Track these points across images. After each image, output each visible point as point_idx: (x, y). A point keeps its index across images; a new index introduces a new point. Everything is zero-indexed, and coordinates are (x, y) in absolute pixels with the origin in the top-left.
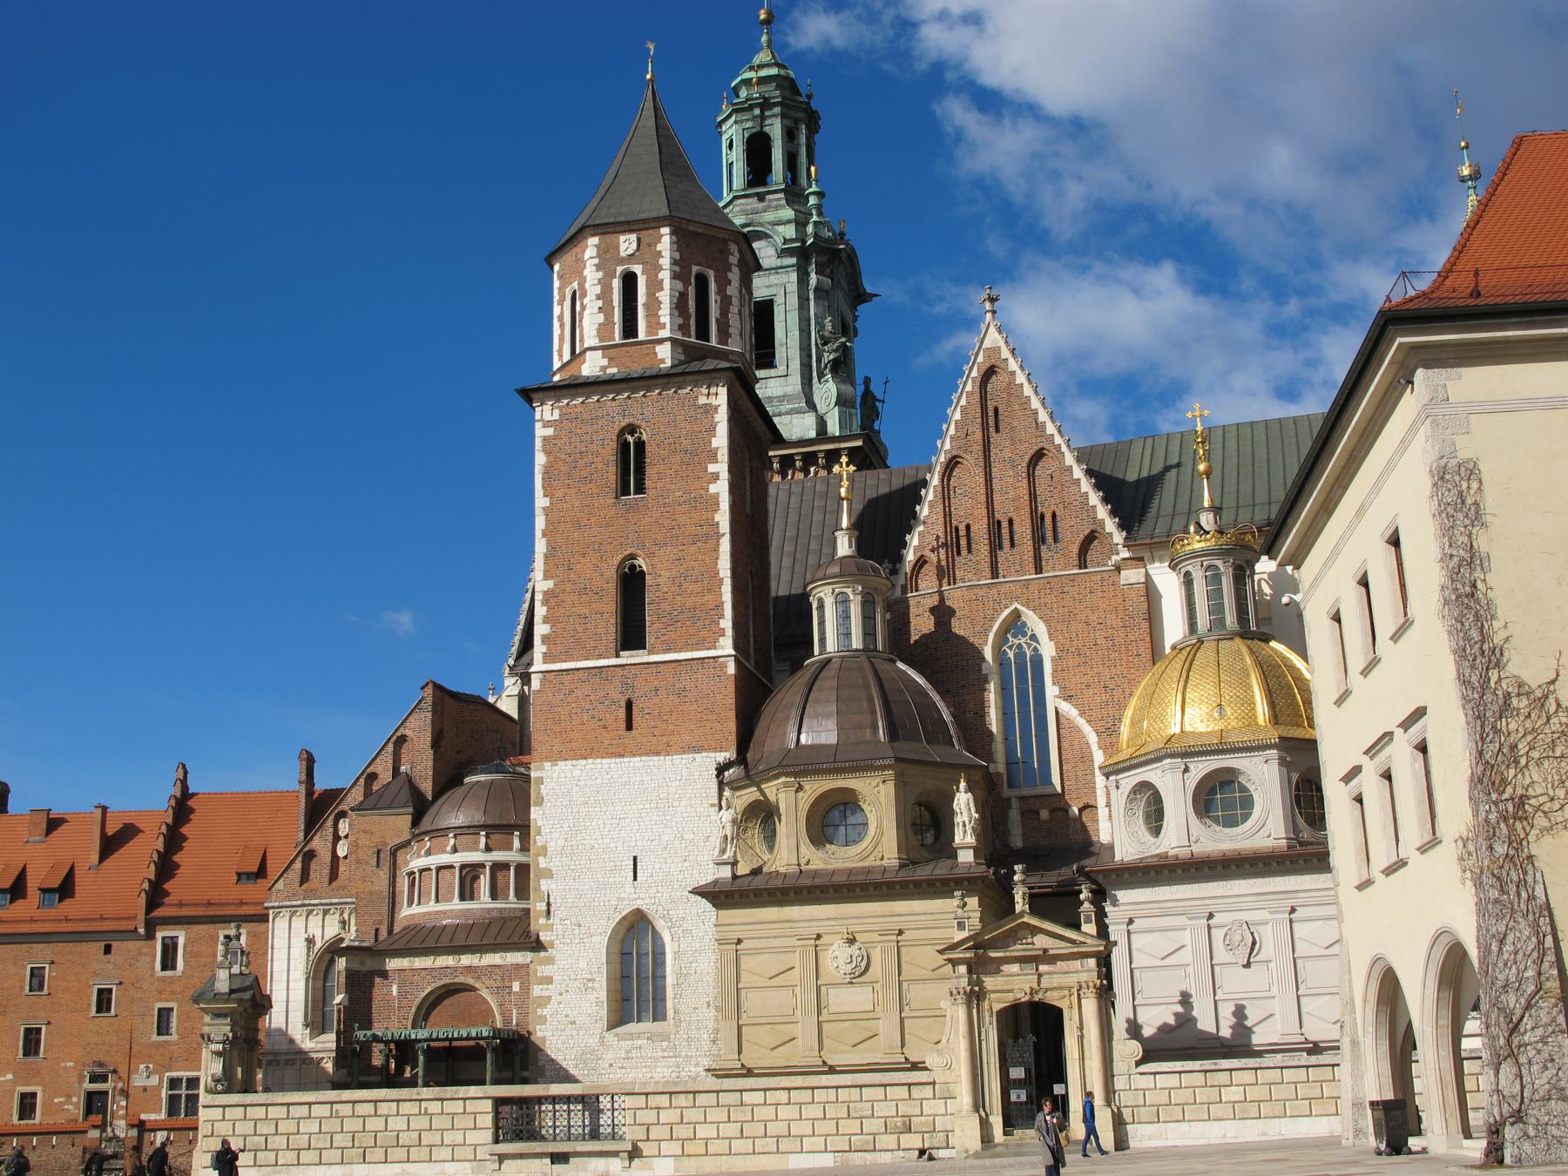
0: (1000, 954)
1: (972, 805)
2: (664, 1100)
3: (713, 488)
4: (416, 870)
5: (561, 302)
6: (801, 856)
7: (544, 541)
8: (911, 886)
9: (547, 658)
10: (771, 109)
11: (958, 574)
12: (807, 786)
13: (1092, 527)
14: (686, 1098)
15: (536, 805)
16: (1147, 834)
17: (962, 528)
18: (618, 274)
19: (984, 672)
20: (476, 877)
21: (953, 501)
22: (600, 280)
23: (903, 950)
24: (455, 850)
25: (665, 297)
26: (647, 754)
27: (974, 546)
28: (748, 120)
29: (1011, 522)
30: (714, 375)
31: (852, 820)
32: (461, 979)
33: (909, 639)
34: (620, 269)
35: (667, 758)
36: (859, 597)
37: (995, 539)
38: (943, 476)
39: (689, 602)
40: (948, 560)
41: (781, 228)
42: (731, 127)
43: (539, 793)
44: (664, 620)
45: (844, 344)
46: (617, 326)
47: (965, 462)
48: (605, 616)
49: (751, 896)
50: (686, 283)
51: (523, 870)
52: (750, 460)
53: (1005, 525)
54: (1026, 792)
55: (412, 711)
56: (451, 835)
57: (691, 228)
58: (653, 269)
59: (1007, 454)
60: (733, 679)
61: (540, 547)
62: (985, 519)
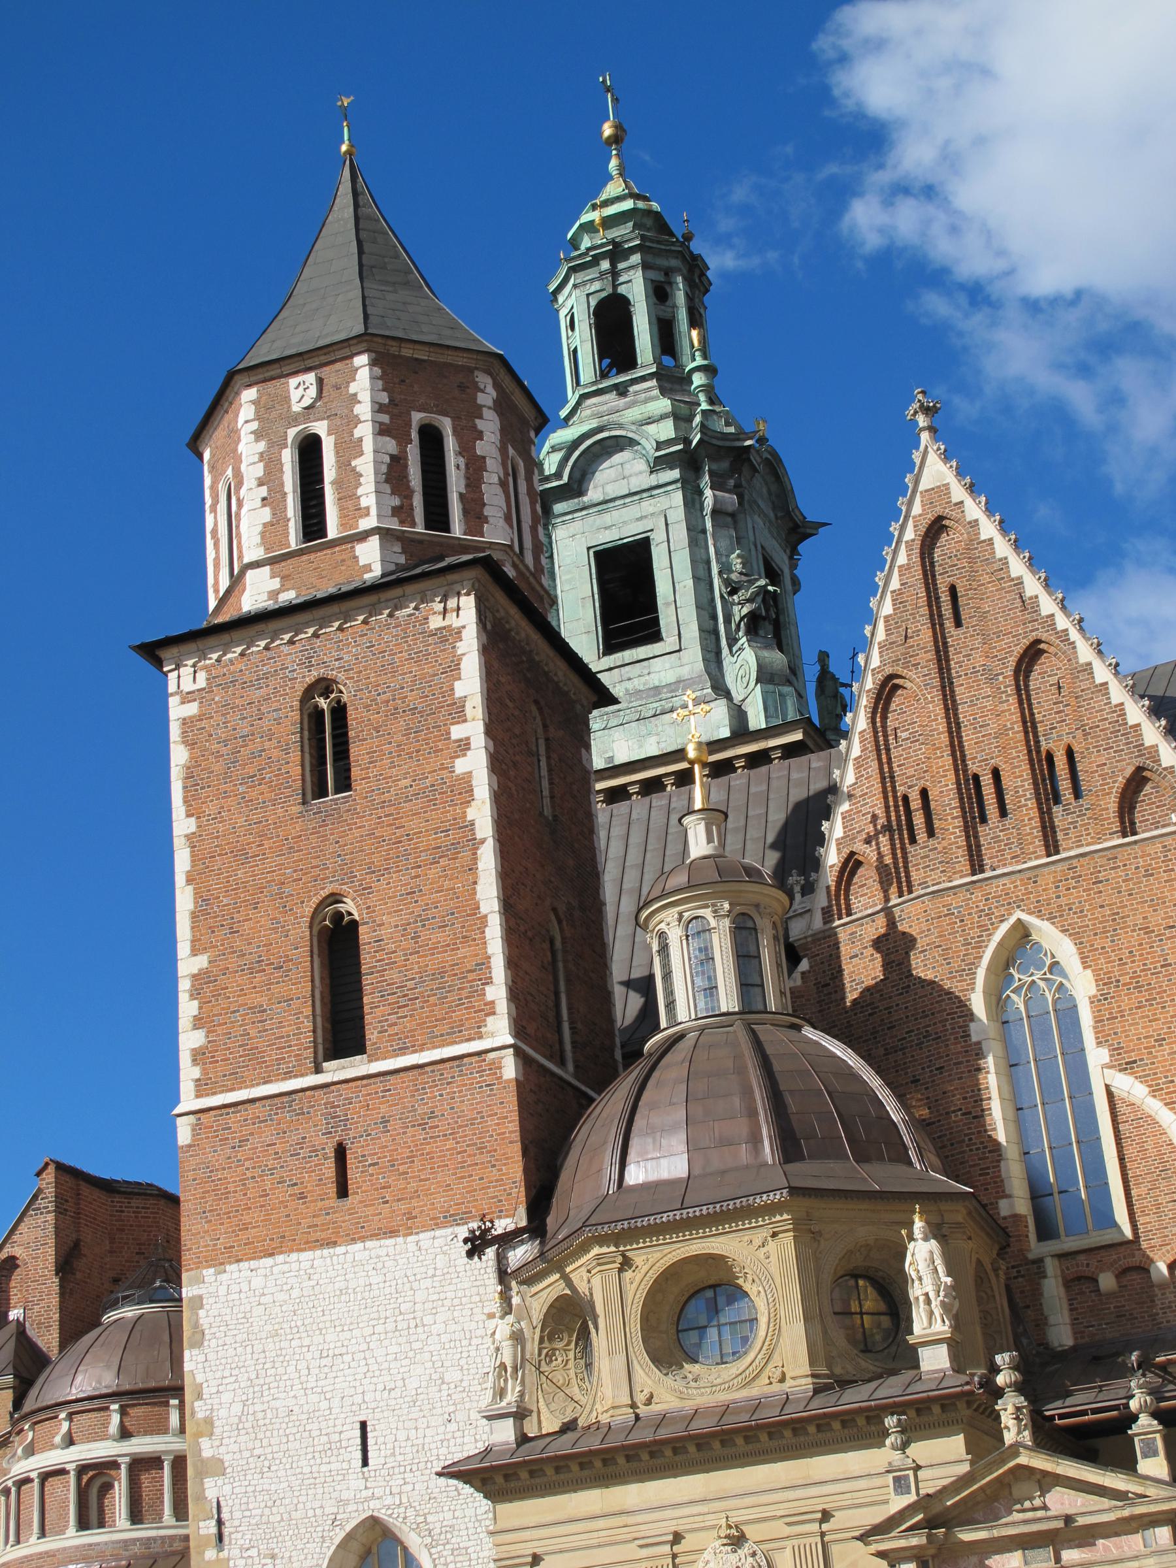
0: (982, 1535)
1: (939, 1262)
3: (461, 766)
5: (214, 509)
6: (637, 1388)
7: (190, 889)
8: (836, 1425)
9: (202, 1089)
10: (626, 259)
11: (914, 875)
12: (638, 1258)
13: (1138, 762)
15: (192, 1346)
19: (974, 1039)
20: (107, 1487)
21: (894, 753)
22: (261, 454)
23: (835, 1549)
24: (70, 1441)
25: (366, 465)
26: (375, 1236)
27: (937, 824)
28: (592, 280)
29: (996, 773)
30: (451, 577)
31: (728, 1314)
33: (844, 998)
34: (292, 433)
35: (410, 1239)
36: (726, 922)
37: (972, 808)
38: (874, 713)
40: (894, 854)
41: (652, 429)
42: (570, 295)
43: (196, 1325)
44: (393, 999)
45: (763, 590)
46: (292, 524)
47: (908, 684)
48: (295, 1004)
49: (550, 1471)
50: (403, 439)
51: (179, 1463)
52: (545, 726)
53: (987, 781)
54: (1069, 1244)
55: (24, 1214)
56: (63, 1415)
57: (407, 352)
59: (978, 660)
60: (513, 1087)
61: (184, 900)
62: (951, 775)
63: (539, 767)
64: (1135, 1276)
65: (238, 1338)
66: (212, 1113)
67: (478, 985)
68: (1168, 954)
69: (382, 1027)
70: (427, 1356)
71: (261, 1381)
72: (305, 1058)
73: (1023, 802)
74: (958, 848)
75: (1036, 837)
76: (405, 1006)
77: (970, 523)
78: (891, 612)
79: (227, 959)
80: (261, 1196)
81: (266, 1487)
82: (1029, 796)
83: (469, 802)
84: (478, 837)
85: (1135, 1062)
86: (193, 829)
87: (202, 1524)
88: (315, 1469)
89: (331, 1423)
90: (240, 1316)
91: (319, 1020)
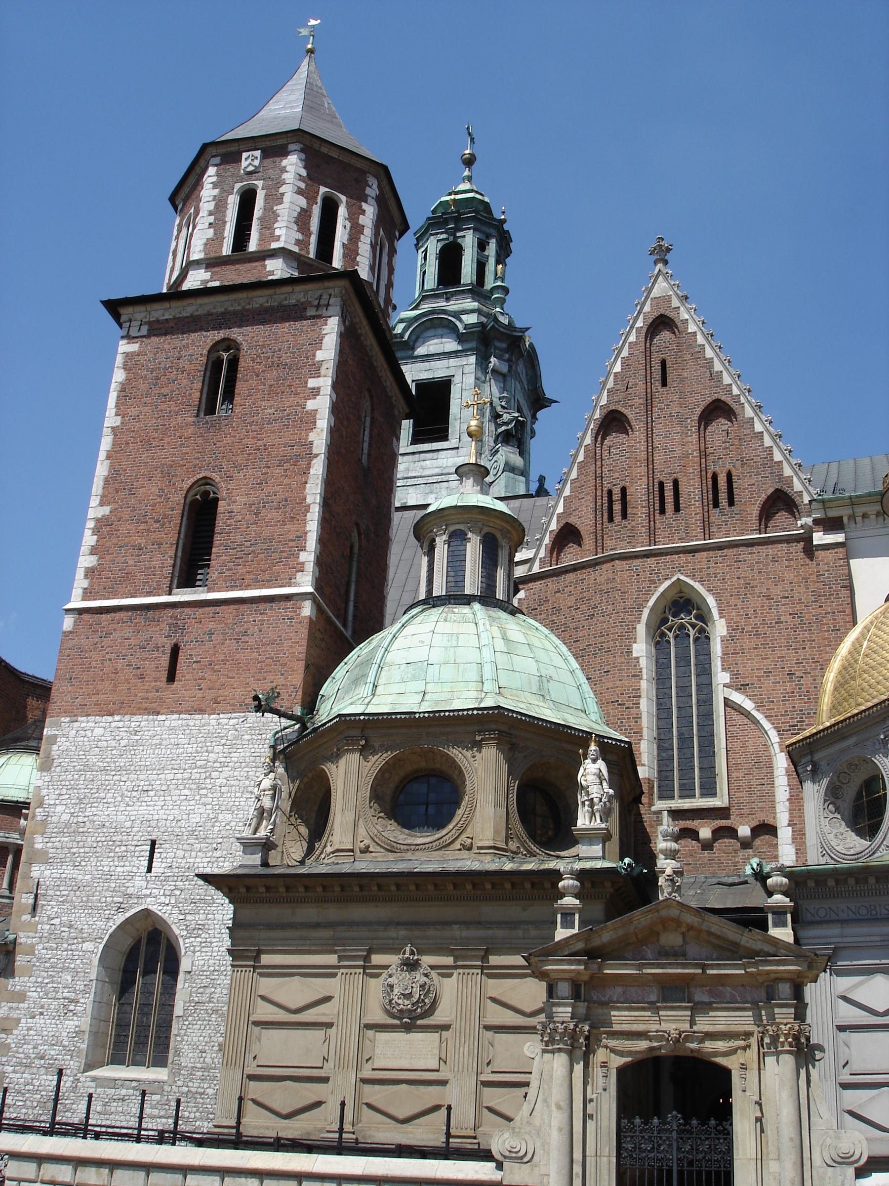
3: (311, 405)
9: (88, 594)
13: (778, 486)
18: (235, 190)
22: (215, 196)
27: (629, 511)
28: (442, 233)
29: (676, 483)
34: (238, 186)
35: (212, 716)
39: (267, 532)
50: (311, 200)
52: (373, 409)
53: (669, 487)
57: (325, 149)
59: (675, 409)
62: (645, 479)
63: (364, 434)
67: (295, 551)
68: (781, 615)
69: (222, 570)
72: (164, 584)
73: (693, 503)
74: (643, 527)
75: (699, 526)
76: (240, 558)
77: (682, 321)
78: (620, 370)
79: (123, 512)
80: (113, 673)
81: (74, 876)
82: (697, 499)
83: (312, 429)
84: (314, 452)
85: (748, 685)
86: (118, 423)
87: (24, 895)
88: (113, 868)
90: (81, 753)
91: (179, 560)
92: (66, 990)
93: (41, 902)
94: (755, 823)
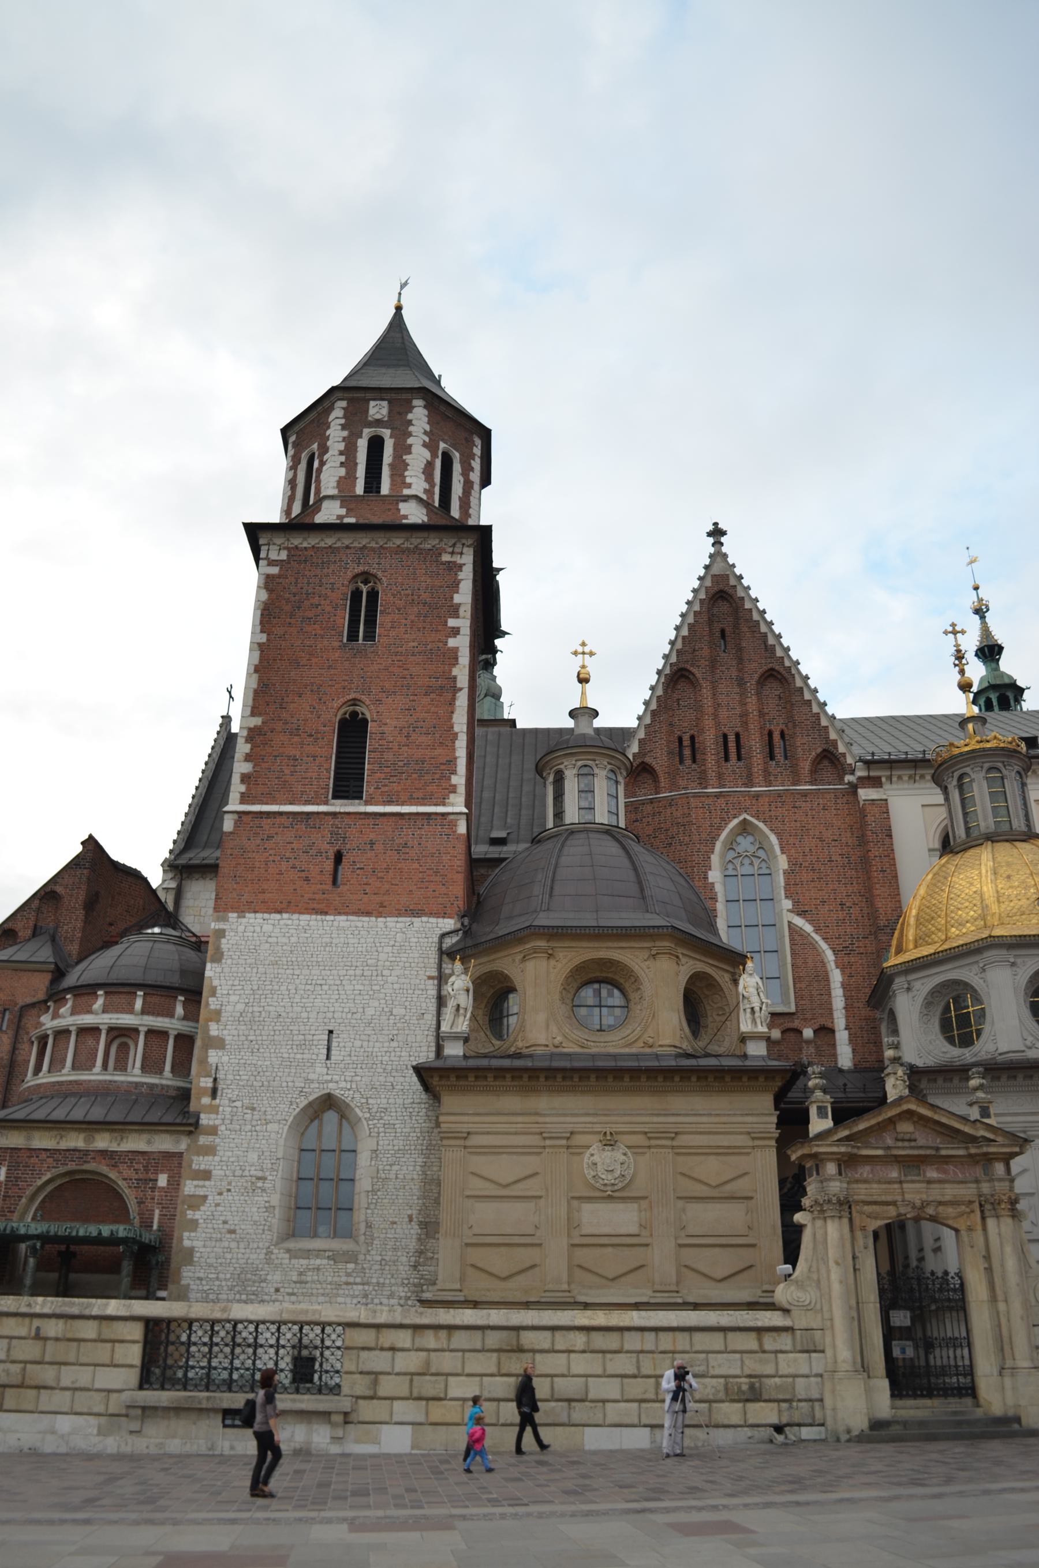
2: (403, 1338)
3: (452, 642)
4: (49, 1032)
9: (244, 799)
13: (825, 746)
14: (436, 1336)
15: (212, 961)
16: (946, 1044)
17: (686, 738)
19: (710, 880)
27: (698, 756)
29: (737, 736)
32: (91, 1166)
35: (380, 919)
50: (434, 455)
53: (732, 738)
58: (402, 432)
64: (792, 1036)
65: (248, 961)
66: (250, 816)
70: (382, 996)
71: (260, 992)
86: (264, 640)
87: (202, 1079)
88: (292, 1056)
89: (307, 1028)
92: (253, 1168)
93: (220, 1087)
94: (816, 1027)
